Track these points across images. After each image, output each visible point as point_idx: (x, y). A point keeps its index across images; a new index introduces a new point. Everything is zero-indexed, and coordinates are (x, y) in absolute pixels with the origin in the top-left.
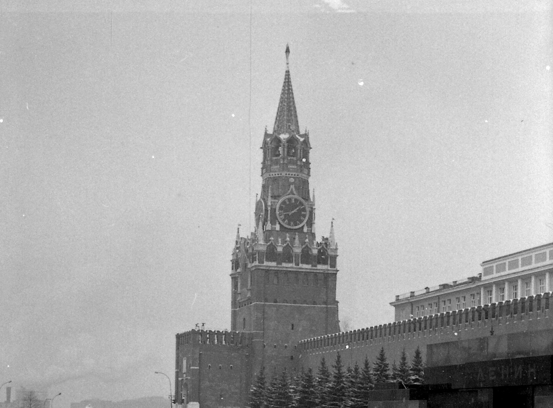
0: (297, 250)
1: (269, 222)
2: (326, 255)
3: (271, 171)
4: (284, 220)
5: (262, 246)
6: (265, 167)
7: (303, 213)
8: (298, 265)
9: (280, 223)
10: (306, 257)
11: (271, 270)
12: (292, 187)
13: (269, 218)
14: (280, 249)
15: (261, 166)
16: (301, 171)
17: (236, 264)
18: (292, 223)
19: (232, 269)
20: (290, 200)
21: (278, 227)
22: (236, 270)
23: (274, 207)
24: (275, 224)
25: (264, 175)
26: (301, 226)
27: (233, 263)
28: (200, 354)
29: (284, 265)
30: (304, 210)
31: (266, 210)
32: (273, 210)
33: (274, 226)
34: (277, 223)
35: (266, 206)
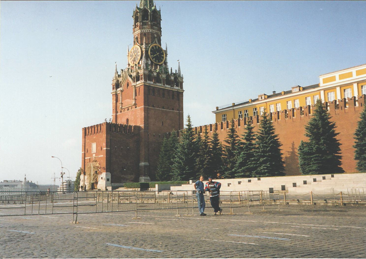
2: (177, 80)
7: (162, 55)
8: (165, 85)
9: (150, 60)
11: (151, 86)
12: (156, 40)
17: (117, 85)
19: (113, 89)
20: (155, 46)
21: (150, 62)
22: (116, 90)
23: (147, 49)
24: (148, 61)
25: (136, 32)
27: (113, 86)
28: (110, 139)
29: (157, 84)
33: (147, 61)
34: (149, 59)
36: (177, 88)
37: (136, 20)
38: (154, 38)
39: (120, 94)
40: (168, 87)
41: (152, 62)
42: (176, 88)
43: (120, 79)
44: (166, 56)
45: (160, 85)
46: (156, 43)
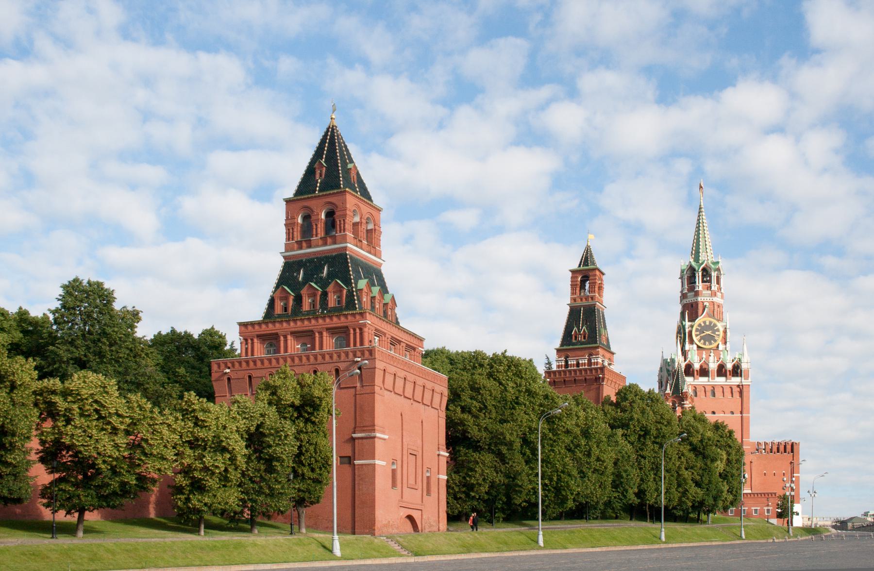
0: (713, 366)
10: (721, 371)
14: (697, 366)
15: (680, 295)
21: (695, 346)
26: (716, 344)
31: (685, 334)
32: (690, 333)
35: (684, 330)
40: (721, 380)
41: (698, 347)
42: (736, 380)
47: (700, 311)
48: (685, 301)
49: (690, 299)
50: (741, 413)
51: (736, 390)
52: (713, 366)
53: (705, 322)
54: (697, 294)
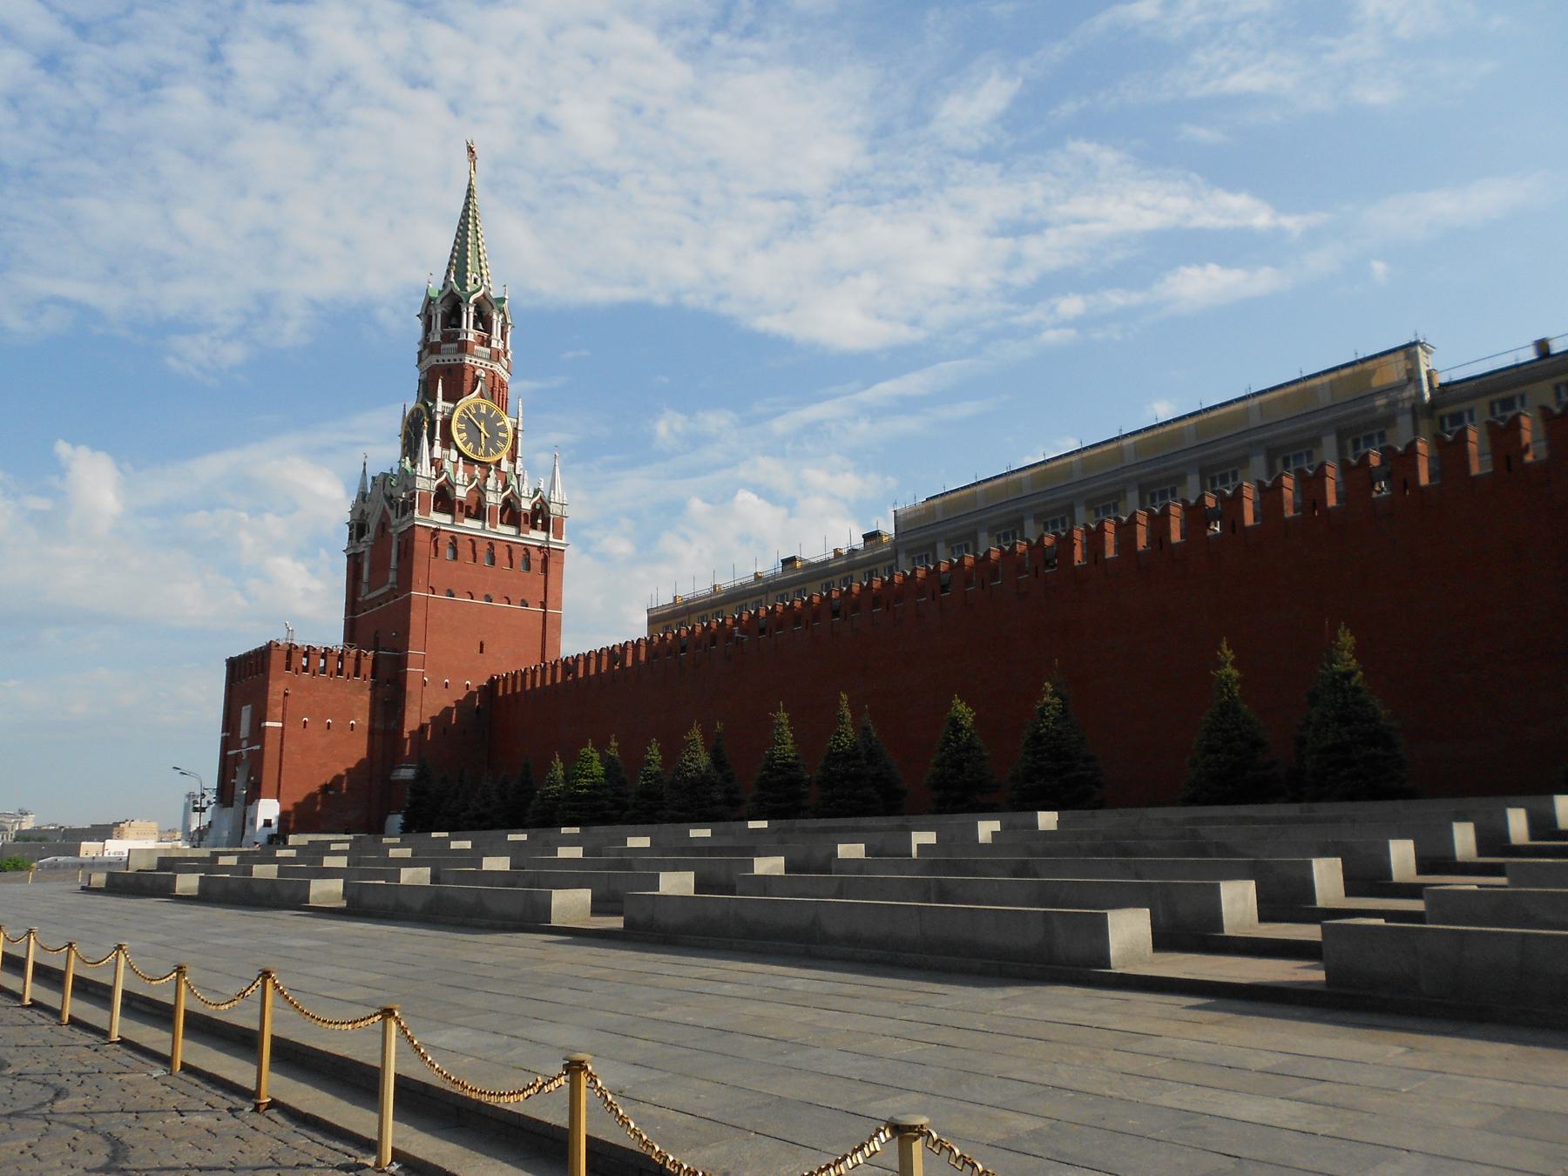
0: (494, 499)
1: (437, 443)
3: (439, 352)
4: (465, 444)
5: (426, 479)
6: (428, 347)
10: (511, 512)
13: (438, 437)
14: (461, 493)
15: (418, 348)
16: (498, 360)
18: (481, 451)
19: (351, 538)
25: (424, 364)
30: (504, 429)
31: (432, 424)
32: (447, 423)
36: (541, 535)
37: (428, 328)
38: (476, 380)
39: (367, 554)
41: (461, 454)
42: (537, 536)
43: (368, 508)
44: (515, 437)
45: (477, 524)
46: (481, 395)
47: (467, 384)
48: (433, 360)
49: (447, 357)
50: (544, 605)
51: (536, 557)
52: (494, 499)
53: (477, 407)
54: (463, 347)
